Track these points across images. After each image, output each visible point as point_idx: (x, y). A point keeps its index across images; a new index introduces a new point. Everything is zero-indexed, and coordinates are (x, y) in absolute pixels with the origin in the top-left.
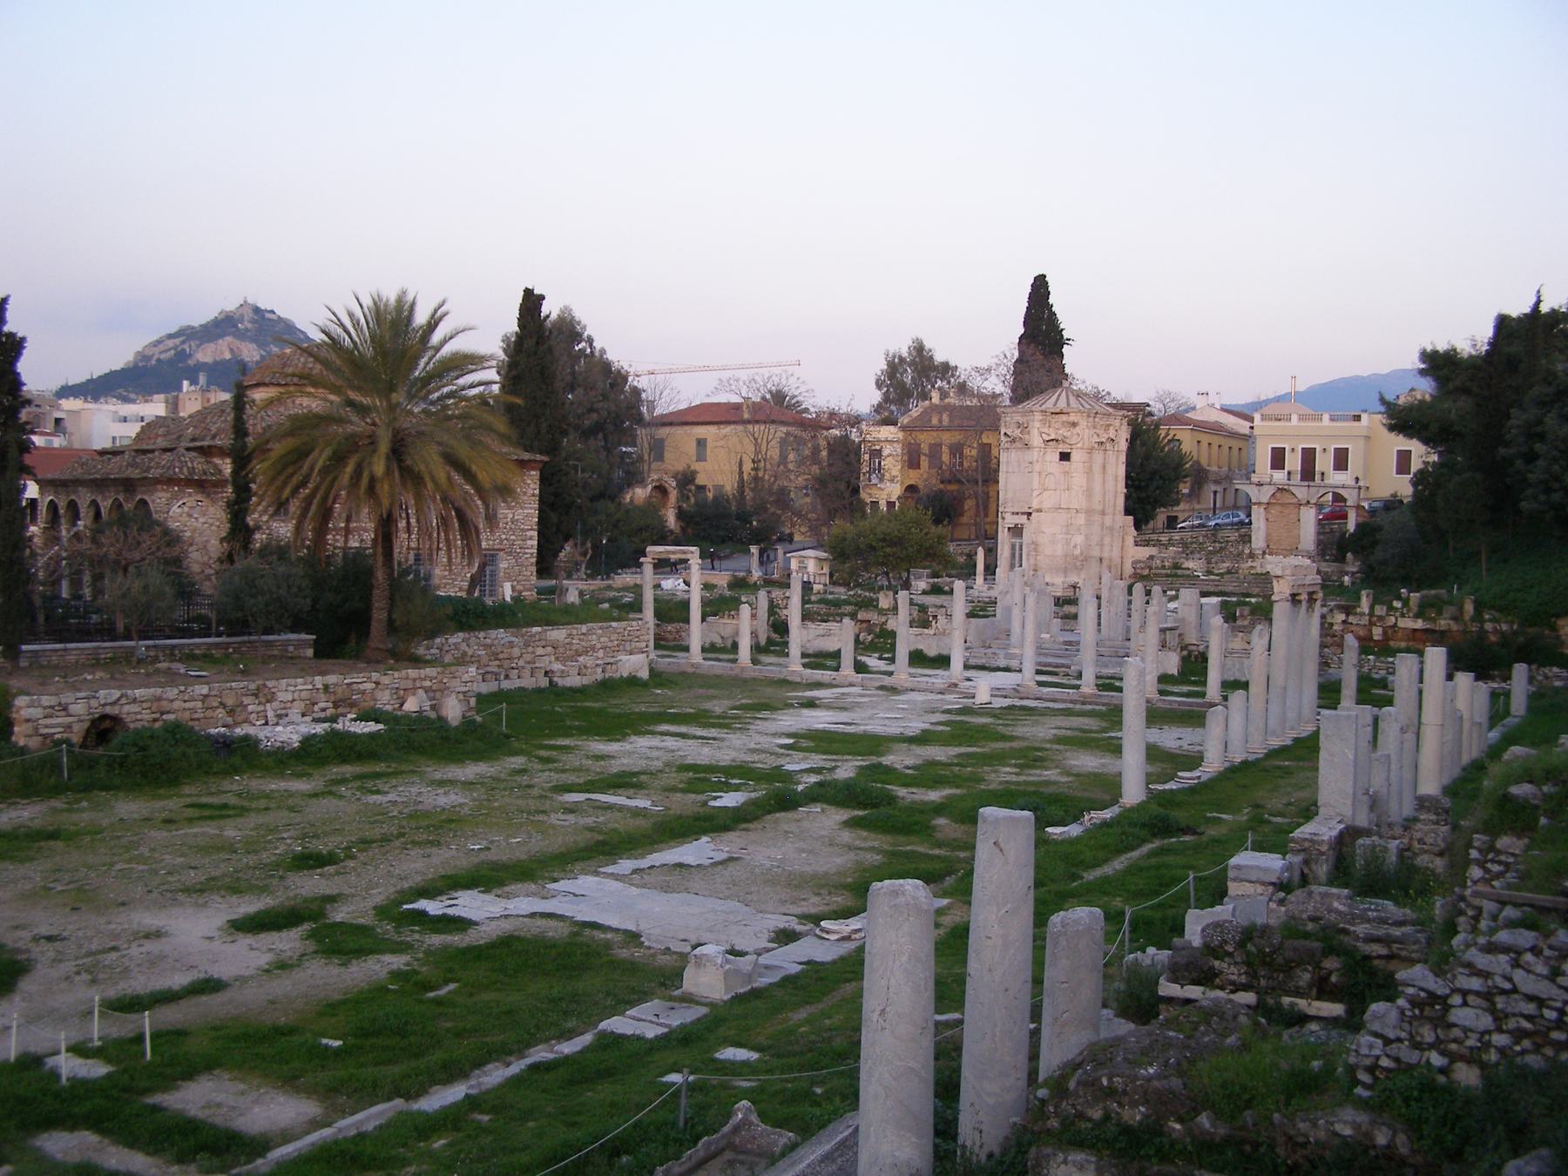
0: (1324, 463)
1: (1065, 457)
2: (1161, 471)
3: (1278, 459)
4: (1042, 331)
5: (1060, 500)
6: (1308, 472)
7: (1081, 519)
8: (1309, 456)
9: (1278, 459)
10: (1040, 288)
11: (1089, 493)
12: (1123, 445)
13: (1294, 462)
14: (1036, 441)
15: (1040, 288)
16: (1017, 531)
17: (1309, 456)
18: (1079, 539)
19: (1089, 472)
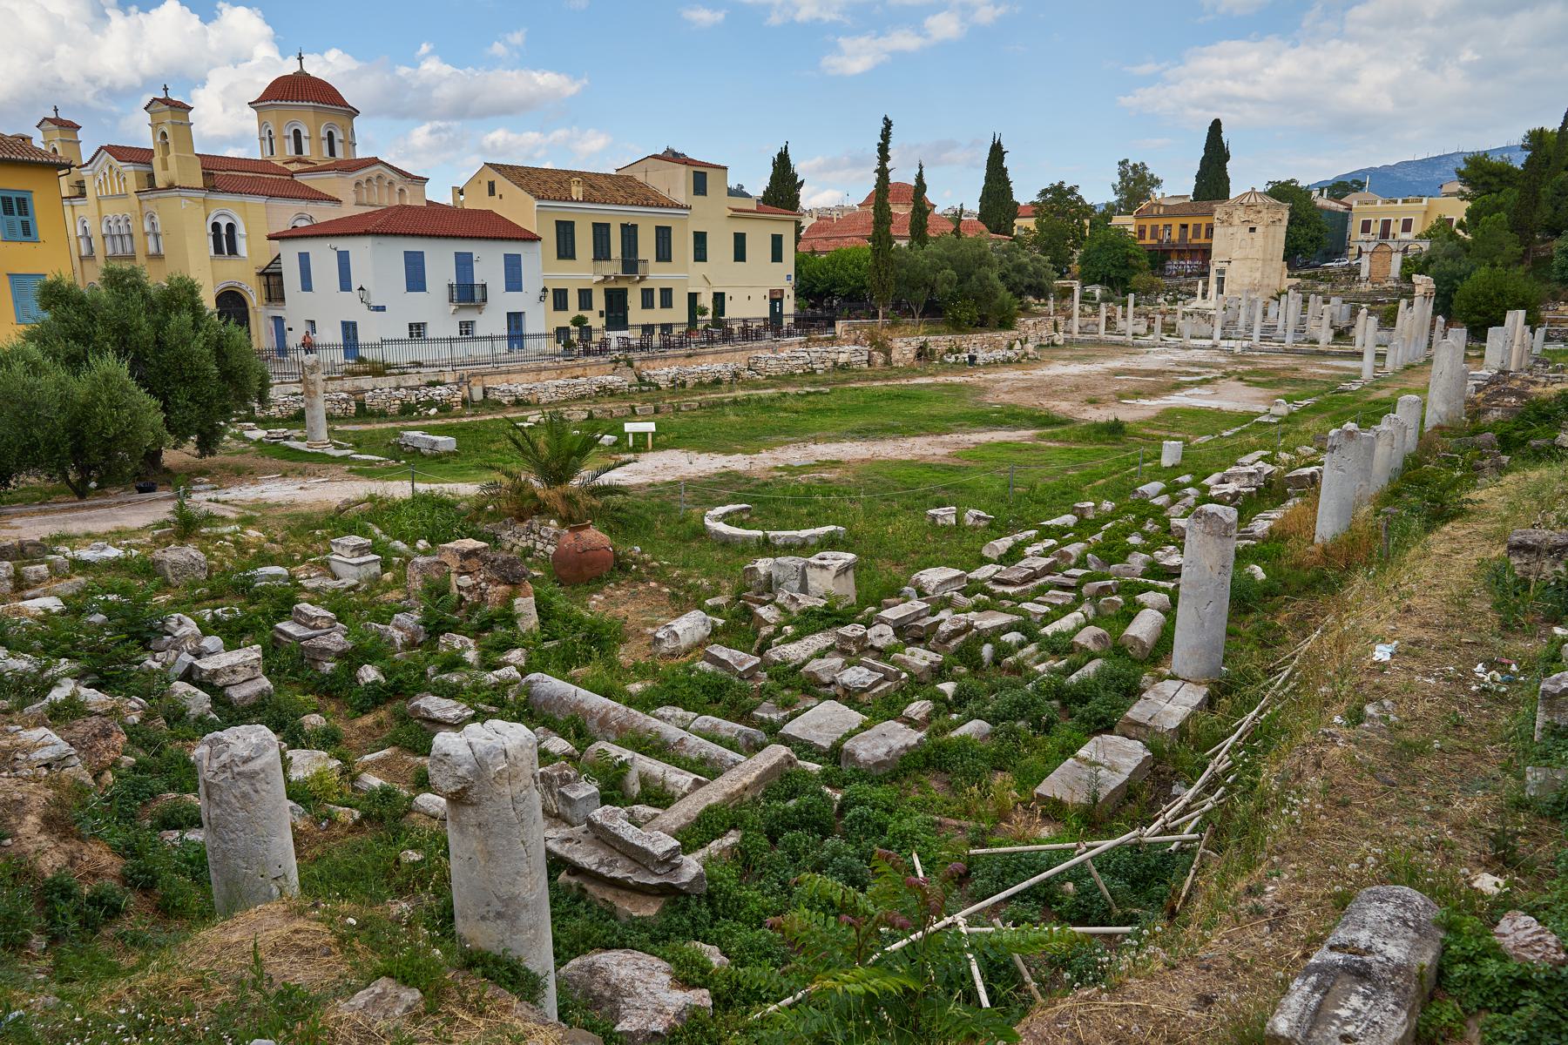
0: (1395, 228)
1: (1252, 230)
2: (1314, 235)
3: (1366, 227)
4: (1216, 154)
5: (1247, 253)
6: (1385, 233)
7: (1260, 264)
8: (1386, 224)
9: (1366, 227)
10: (1216, 127)
11: (1264, 251)
12: (1285, 223)
13: (1376, 228)
14: (1236, 221)
15: (1216, 127)
16: (1221, 271)
17: (1386, 224)
18: (1258, 275)
19: (1266, 237)
